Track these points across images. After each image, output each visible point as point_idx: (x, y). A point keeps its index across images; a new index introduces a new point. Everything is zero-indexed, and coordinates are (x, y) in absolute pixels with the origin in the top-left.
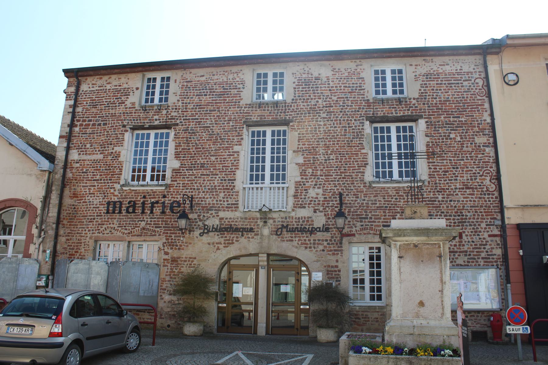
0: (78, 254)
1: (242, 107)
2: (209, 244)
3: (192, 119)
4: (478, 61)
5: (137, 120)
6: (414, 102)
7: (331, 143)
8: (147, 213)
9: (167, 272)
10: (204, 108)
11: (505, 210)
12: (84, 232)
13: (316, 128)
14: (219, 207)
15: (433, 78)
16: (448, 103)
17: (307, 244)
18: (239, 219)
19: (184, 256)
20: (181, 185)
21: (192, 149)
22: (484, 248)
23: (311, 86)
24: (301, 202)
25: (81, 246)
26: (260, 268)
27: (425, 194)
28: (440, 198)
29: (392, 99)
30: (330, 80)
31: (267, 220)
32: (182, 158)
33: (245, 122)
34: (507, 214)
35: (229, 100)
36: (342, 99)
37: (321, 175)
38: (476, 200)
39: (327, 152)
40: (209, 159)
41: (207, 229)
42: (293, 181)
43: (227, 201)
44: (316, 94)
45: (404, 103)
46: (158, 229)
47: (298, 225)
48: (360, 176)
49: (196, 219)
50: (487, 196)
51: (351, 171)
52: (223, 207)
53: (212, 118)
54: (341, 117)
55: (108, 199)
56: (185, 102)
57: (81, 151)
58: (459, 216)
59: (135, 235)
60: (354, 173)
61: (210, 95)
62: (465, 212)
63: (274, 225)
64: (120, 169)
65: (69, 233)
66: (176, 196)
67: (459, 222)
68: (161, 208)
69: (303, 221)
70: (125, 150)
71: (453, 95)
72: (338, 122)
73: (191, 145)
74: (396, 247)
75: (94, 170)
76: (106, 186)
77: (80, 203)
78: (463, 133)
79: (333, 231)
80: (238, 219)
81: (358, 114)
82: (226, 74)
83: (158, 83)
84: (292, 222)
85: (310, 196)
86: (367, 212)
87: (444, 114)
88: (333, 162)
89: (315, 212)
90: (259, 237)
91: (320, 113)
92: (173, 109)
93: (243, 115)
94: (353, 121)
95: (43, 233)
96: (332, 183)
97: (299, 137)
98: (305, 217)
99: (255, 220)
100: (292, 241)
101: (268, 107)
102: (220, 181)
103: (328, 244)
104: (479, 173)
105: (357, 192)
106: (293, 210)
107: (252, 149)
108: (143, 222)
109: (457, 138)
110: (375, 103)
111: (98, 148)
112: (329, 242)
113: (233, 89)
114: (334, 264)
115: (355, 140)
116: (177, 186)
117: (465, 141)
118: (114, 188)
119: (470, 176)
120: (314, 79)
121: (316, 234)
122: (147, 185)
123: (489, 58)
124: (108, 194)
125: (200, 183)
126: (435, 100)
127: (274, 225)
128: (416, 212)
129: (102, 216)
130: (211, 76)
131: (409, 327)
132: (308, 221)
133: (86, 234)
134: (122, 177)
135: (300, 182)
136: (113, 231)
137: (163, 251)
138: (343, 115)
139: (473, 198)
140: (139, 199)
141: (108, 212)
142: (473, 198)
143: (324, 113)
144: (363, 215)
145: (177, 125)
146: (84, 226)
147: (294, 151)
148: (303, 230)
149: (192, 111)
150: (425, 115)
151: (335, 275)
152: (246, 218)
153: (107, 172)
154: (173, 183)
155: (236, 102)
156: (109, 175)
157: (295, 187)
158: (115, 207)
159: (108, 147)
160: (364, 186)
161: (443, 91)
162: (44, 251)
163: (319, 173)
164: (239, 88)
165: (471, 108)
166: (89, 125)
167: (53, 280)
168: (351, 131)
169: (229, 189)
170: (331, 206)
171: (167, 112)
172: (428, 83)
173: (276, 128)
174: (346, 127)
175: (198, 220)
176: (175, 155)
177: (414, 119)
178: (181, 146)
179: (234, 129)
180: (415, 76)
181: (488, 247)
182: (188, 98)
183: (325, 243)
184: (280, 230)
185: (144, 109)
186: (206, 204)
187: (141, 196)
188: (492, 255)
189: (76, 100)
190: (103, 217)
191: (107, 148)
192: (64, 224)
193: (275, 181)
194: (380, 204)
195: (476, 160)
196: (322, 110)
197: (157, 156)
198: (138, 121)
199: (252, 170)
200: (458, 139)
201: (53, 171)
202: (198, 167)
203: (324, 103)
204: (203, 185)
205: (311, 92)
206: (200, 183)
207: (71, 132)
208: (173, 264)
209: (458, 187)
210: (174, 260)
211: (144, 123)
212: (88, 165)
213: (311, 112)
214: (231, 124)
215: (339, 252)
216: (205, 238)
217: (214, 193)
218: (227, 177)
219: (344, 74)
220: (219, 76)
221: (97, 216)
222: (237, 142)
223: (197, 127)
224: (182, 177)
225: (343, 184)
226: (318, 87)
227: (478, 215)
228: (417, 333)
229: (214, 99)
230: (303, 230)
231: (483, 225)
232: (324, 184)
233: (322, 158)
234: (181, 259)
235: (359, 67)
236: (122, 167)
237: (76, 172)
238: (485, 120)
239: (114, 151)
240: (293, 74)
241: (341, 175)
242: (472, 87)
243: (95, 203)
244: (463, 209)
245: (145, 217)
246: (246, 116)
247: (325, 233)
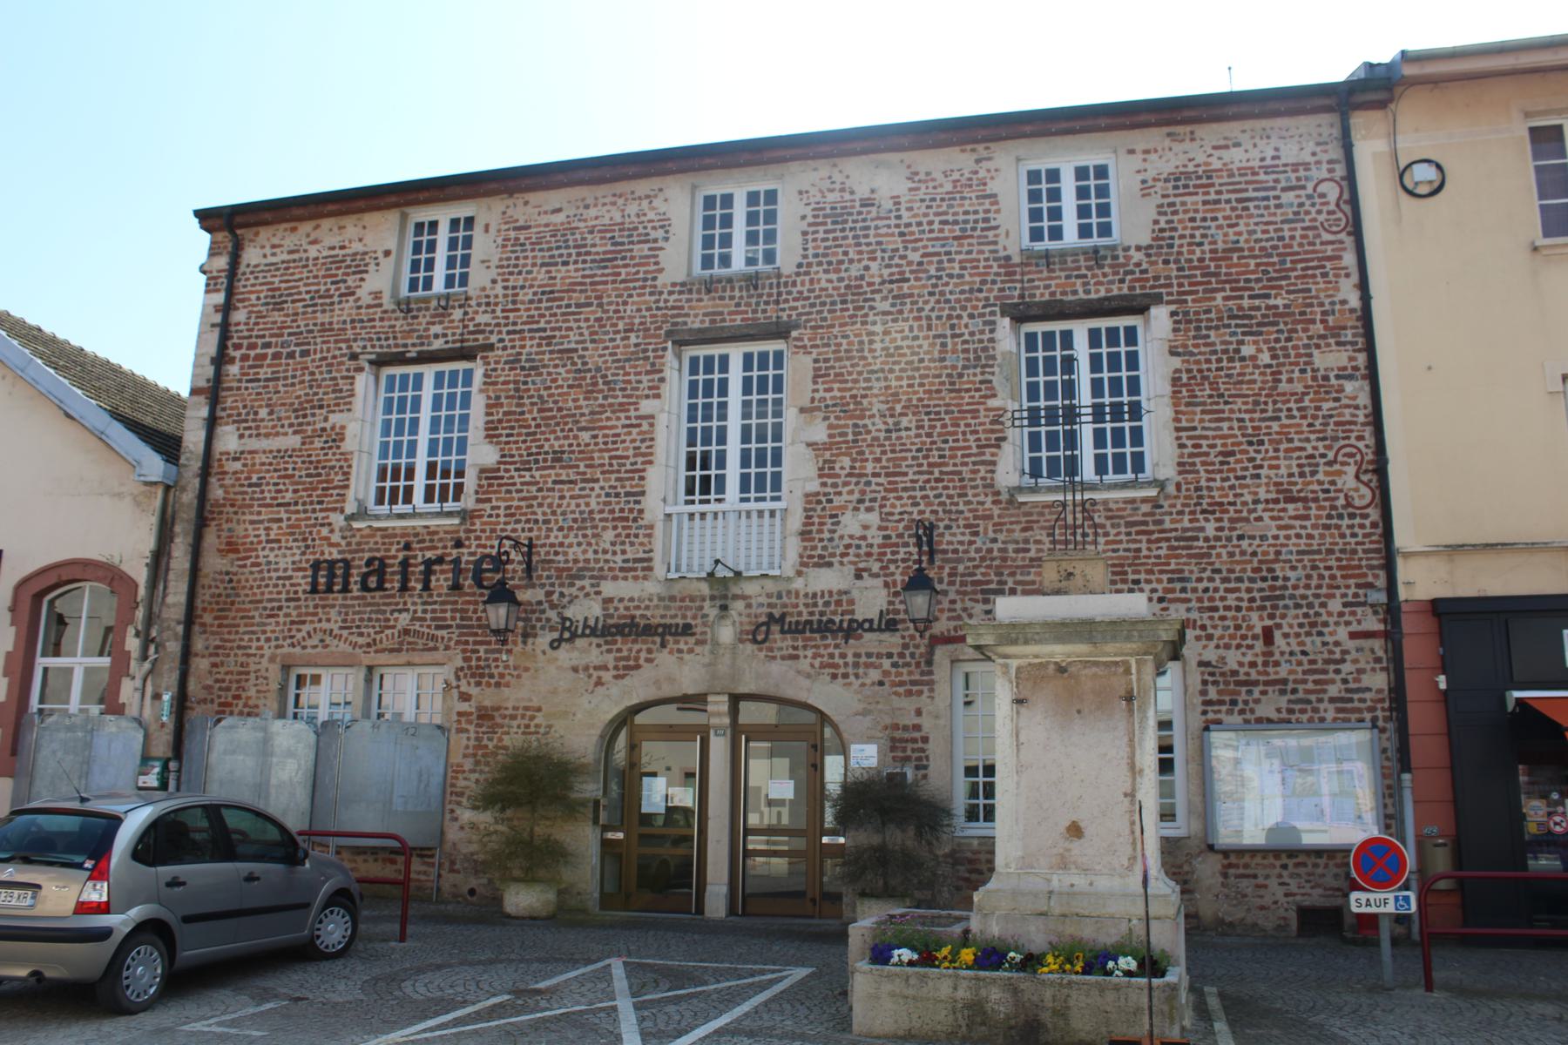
0: (241, 703)
1: (661, 293)
2: (575, 670)
3: (530, 331)
4: (1326, 131)
5: (387, 339)
6: (1137, 256)
7: (905, 383)
9: (467, 747)
10: (562, 299)
11: (1400, 562)
12: (255, 644)
13: (861, 343)
14: (601, 569)
15: (1195, 186)
16: (1235, 256)
17: (836, 666)
18: (655, 602)
19: (510, 705)
20: (502, 512)
21: (531, 412)
22: (1337, 672)
23: (850, 224)
24: (819, 552)
26: (712, 732)
27: (1167, 518)
28: (1211, 529)
29: (1075, 253)
30: (903, 207)
31: (728, 602)
32: (504, 439)
33: (669, 334)
34: (1404, 571)
35: (628, 274)
36: (935, 259)
37: (875, 475)
38: (1316, 533)
39: (892, 409)
40: (576, 437)
41: (569, 629)
42: (799, 494)
43: (624, 552)
44: (864, 248)
45: (1109, 261)
46: (444, 633)
47: (812, 614)
48: (982, 474)
49: (540, 603)
50: (1346, 522)
51: (958, 461)
52: (611, 569)
53: (583, 324)
54: (932, 310)
56: (510, 284)
58: (1264, 579)
59: (383, 651)
60: (966, 464)
61: (576, 262)
63: (749, 615)
65: (218, 647)
67: (1263, 599)
69: (827, 604)
71: (1251, 233)
72: (924, 322)
73: (526, 401)
74: (1006, 673)
78: (1277, 340)
79: (907, 629)
80: (650, 600)
81: (978, 300)
82: (620, 201)
84: (797, 606)
85: (846, 532)
86: (1001, 574)
87: (1223, 290)
88: (908, 437)
89: (858, 576)
90: (707, 647)
91: (873, 300)
92: (479, 305)
93: (664, 315)
94: (965, 320)
95: (152, 649)
96: (905, 495)
97: (815, 369)
98: (830, 593)
100: (796, 657)
101: (733, 289)
102: (603, 499)
103: (895, 665)
104: (1323, 456)
105: (975, 518)
106: (799, 573)
107: (692, 408)
108: (405, 615)
109: (1260, 356)
110: (1027, 265)
112: (896, 659)
113: (639, 242)
114: (911, 720)
115: (971, 371)
116: (490, 516)
117: (1283, 364)
119: (1299, 466)
120: (857, 204)
121: (861, 637)
123: (1358, 120)
125: (550, 505)
126: (1198, 250)
127: (749, 615)
128: (1070, 574)
129: (298, 599)
130: (581, 210)
131: (1036, 895)
132: (839, 603)
133: (260, 648)
135: (818, 494)
136: (328, 640)
137: (455, 691)
138: (938, 302)
139: (1304, 527)
140: (393, 552)
141: (314, 590)
142: (1304, 527)
143: (885, 299)
144: (988, 582)
145: (491, 347)
147: (802, 410)
148: (825, 628)
149: (528, 310)
150: (1169, 294)
151: (913, 750)
152: (672, 598)
154: (481, 506)
155: (645, 280)
156: (315, 489)
157: (806, 510)
158: (331, 576)
159: (313, 415)
160: (994, 502)
161: (1221, 222)
162: (157, 696)
163: (870, 467)
164: (655, 241)
166: (264, 357)
167: (179, 771)
168: (959, 347)
169: (626, 519)
170: (904, 561)
171: (466, 313)
172: (1178, 200)
173: (755, 348)
174: (945, 336)
175: (546, 605)
176: (487, 429)
177: (1138, 307)
178: (502, 405)
179: (640, 353)
180: (1144, 182)
181: (1347, 667)
182: (520, 273)
183: (886, 663)
184: (764, 628)
185: (405, 307)
186: (567, 561)
189: (230, 292)
190: (302, 603)
191: (310, 419)
192: (203, 625)
193: (753, 495)
194: (1039, 550)
195: (1315, 417)
196: (879, 291)
198: (391, 342)
199: (691, 465)
200: (1265, 358)
201: (176, 482)
202: (545, 460)
203: (886, 272)
205: (851, 241)
206: (550, 505)
207: (218, 378)
209: (1263, 496)
210: (485, 715)
211: (405, 345)
212: (263, 464)
213: (850, 298)
214: (633, 340)
215: (925, 689)
216: (565, 655)
217: (589, 532)
219: (941, 186)
220: (602, 209)
222: (650, 388)
223: (543, 353)
225: (936, 496)
226: (868, 228)
227: (1321, 577)
228: (1057, 911)
229: (587, 272)
230: (825, 628)
231: (1335, 605)
232: (884, 498)
233: (877, 426)
235: (985, 164)
236: (350, 466)
238: (1343, 302)
239: (328, 425)
240: (800, 193)
241: (932, 473)
242: (1307, 207)
243: (282, 566)
244: (1276, 561)
245: (409, 601)
246: (673, 316)
247: (886, 636)
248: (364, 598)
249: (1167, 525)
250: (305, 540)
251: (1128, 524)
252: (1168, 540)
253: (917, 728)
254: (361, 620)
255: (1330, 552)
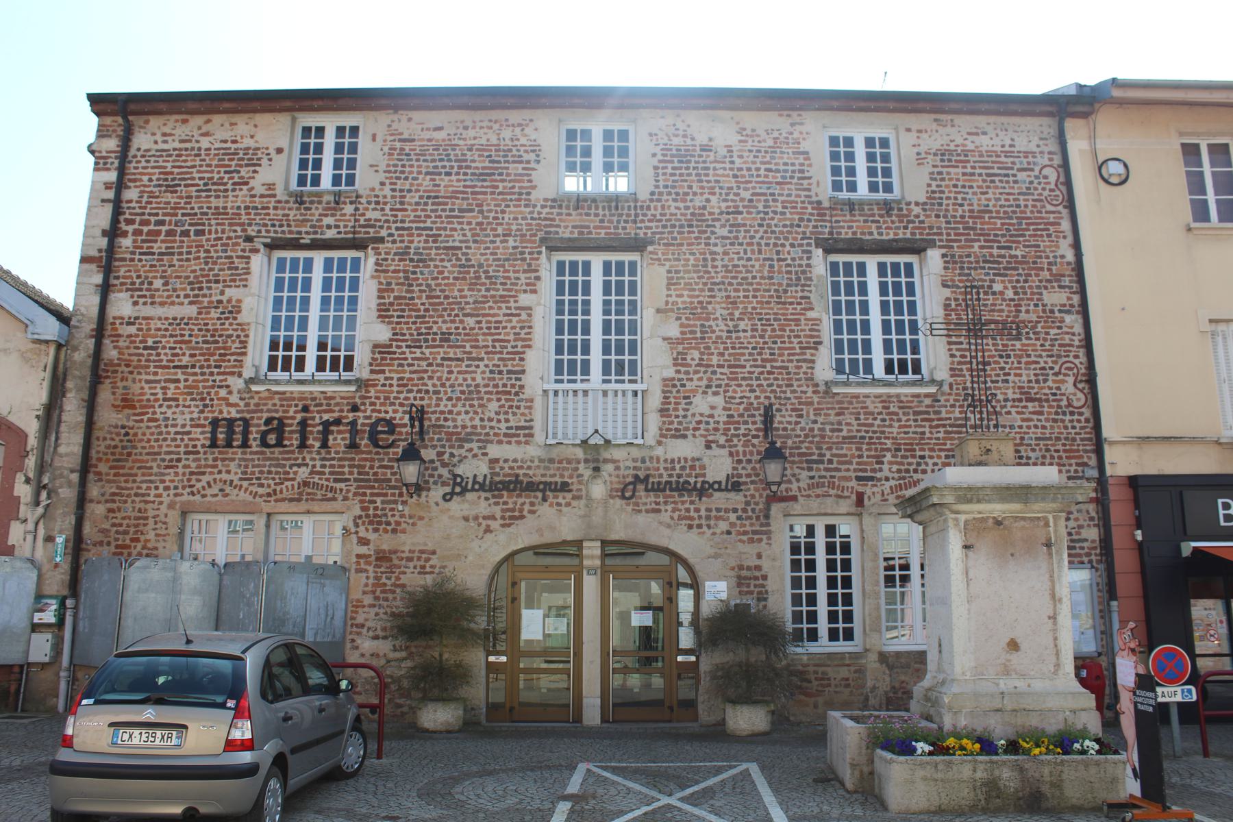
0: (139, 546)
1: (535, 206)
2: (466, 519)
3: (417, 229)
4: (1046, 130)
5: (281, 226)
6: (917, 210)
7: (741, 294)
8: (313, 446)
9: (366, 585)
10: (446, 204)
11: (1106, 447)
12: (153, 492)
13: (705, 260)
14: (487, 434)
15: (956, 161)
16: (987, 216)
17: (692, 518)
18: (536, 463)
19: (407, 548)
20: (395, 382)
21: (420, 298)
23: (692, 165)
24: (675, 426)
25: (145, 525)
26: (585, 572)
27: (943, 410)
29: (870, 203)
30: (735, 154)
31: (600, 465)
32: (395, 320)
33: (543, 240)
34: (1110, 454)
35: (504, 188)
36: (763, 198)
37: (720, 366)
38: (1048, 424)
39: (732, 314)
40: (462, 322)
42: (657, 378)
43: (507, 421)
44: (705, 184)
45: (895, 212)
46: (342, 485)
47: (670, 476)
48: (804, 369)
50: (1068, 417)
51: (785, 358)
52: (496, 435)
53: (465, 227)
54: (762, 238)
55: (213, 412)
56: (398, 187)
57: (139, 296)
59: (283, 500)
60: (791, 361)
61: (457, 174)
63: (618, 476)
64: (241, 342)
65: (114, 494)
66: (383, 409)
68: (348, 435)
69: (683, 468)
70: (253, 295)
71: (998, 200)
72: (755, 247)
73: (416, 289)
74: (957, 525)
75: (175, 342)
76: (207, 381)
77: (142, 421)
78: (1018, 281)
79: (749, 490)
80: (532, 461)
81: (797, 233)
82: (496, 127)
83: (329, 141)
84: (658, 469)
85: (698, 410)
86: (821, 448)
87: (979, 241)
88: (746, 337)
89: (708, 447)
90: (583, 502)
91: (714, 226)
92: (369, 203)
93: (539, 225)
94: (788, 248)
95: (44, 495)
96: (744, 383)
97: (669, 278)
98: (686, 460)
99: (573, 465)
100: (659, 511)
101: (597, 208)
102: (488, 375)
103: (739, 518)
104: (1051, 368)
105: (800, 403)
106: (659, 443)
107: (560, 303)
108: (304, 469)
110: (834, 209)
111: (184, 289)
112: (740, 513)
113: (514, 162)
114: (754, 562)
115: (794, 288)
116: (384, 385)
117: (1022, 299)
118: (228, 386)
119: (1035, 375)
120: (698, 148)
121: (711, 495)
122: (313, 381)
123: (1069, 124)
124: (212, 400)
125: (440, 379)
126: (960, 209)
127: (618, 476)
128: (989, 450)
129: (198, 453)
130: (461, 130)
131: (992, 696)
132: (693, 468)
133: (160, 496)
134: (248, 361)
135: (673, 379)
136: (228, 489)
137: (354, 537)
138: (766, 232)
139: (1039, 420)
140: (291, 413)
141: (214, 444)
142: (1039, 420)
143: (723, 226)
144: (813, 454)
145: (382, 240)
146: (152, 478)
147: (658, 311)
148: (682, 488)
149: (416, 210)
150: (941, 240)
151: (755, 586)
152: (551, 461)
153: (208, 349)
154: (374, 376)
155: (520, 194)
157: (663, 392)
158: (230, 432)
159: (209, 288)
160: (814, 392)
161: (975, 189)
162: (49, 539)
163: (715, 360)
164: (528, 162)
166: (158, 233)
167: (76, 608)
168: (784, 269)
169: (509, 393)
170: (744, 435)
171: (357, 209)
172: (945, 170)
173: (613, 257)
174: (772, 260)
175: (438, 464)
177: (917, 249)
178: (393, 291)
179: (517, 255)
180: (918, 154)
182: (406, 178)
183: (733, 517)
184: (631, 487)
185: (299, 199)
186: (456, 427)
187: (296, 406)
189: (122, 171)
190: (201, 456)
191: (205, 291)
192: (99, 473)
193: (613, 377)
194: (849, 431)
195: (1046, 340)
196: (719, 220)
197: (332, 314)
198: (285, 228)
200: (1010, 294)
201: (67, 342)
203: (723, 205)
204: (448, 384)
205: (693, 178)
206: (440, 379)
207: (111, 249)
208: (380, 567)
209: (1010, 396)
210: (382, 557)
211: (300, 233)
212: (159, 329)
213: (695, 223)
214: (511, 243)
215: (764, 537)
216: (456, 506)
217: (476, 403)
218: (505, 366)
219: (765, 141)
220: (481, 131)
221: (186, 453)
222: (527, 284)
223: (431, 248)
224: (396, 362)
225: (769, 385)
226: (707, 169)
227: (1052, 457)
228: (1009, 708)
229: (468, 183)
230: (682, 488)
232: (727, 385)
233: (720, 327)
234: (399, 554)
235: (798, 128)
236: (247, 336)
237: (128, 348)
238: (1062, 257)
239: (224, 298)
240: (651, 135)
241: (765, 367)
242: (1035, 185)
243: (180, 422)
244: (1021, 444)
245: (308, 457)
246: (546, 226)
247: (732, 495)
248: (263, 453)
249: (944, 415)
250: (203, 399)
251: (915, 413)
252: (944, 426)
253: (758, 568)
254: (261, 472)
255: (1058, 439)
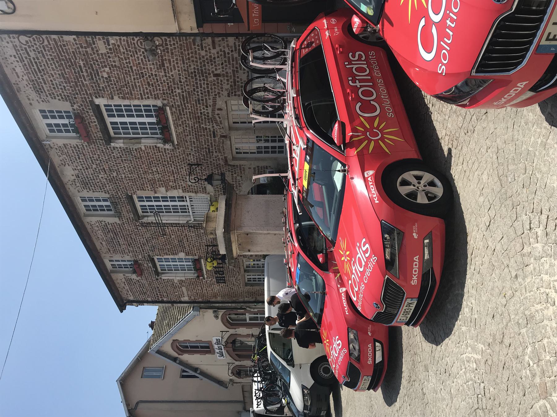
6: (75, 107)
22: (228, 53)
27: (177, 104)
28: (178, 91)
38: (175, 58)
50: (169, 46)
58: (195, 76)
62: (191, 69)
67: (203, 76)
109: (106, 71)
142: (173, 61)
145: (149, 255)
150: (89, 98)
165: (64, 53)
181: (227, 50)
183: (234, 175)
188: (235, 47)
194: (193, 138)
200: (107, 69)
227: (192, 57)
231: (203, 53)
233: (157, 176)
244: (188, 71)
249: (179, 103)
251: (181, 114)
252: (184, 104)
253: (254, 168)
255: (182, 53)
